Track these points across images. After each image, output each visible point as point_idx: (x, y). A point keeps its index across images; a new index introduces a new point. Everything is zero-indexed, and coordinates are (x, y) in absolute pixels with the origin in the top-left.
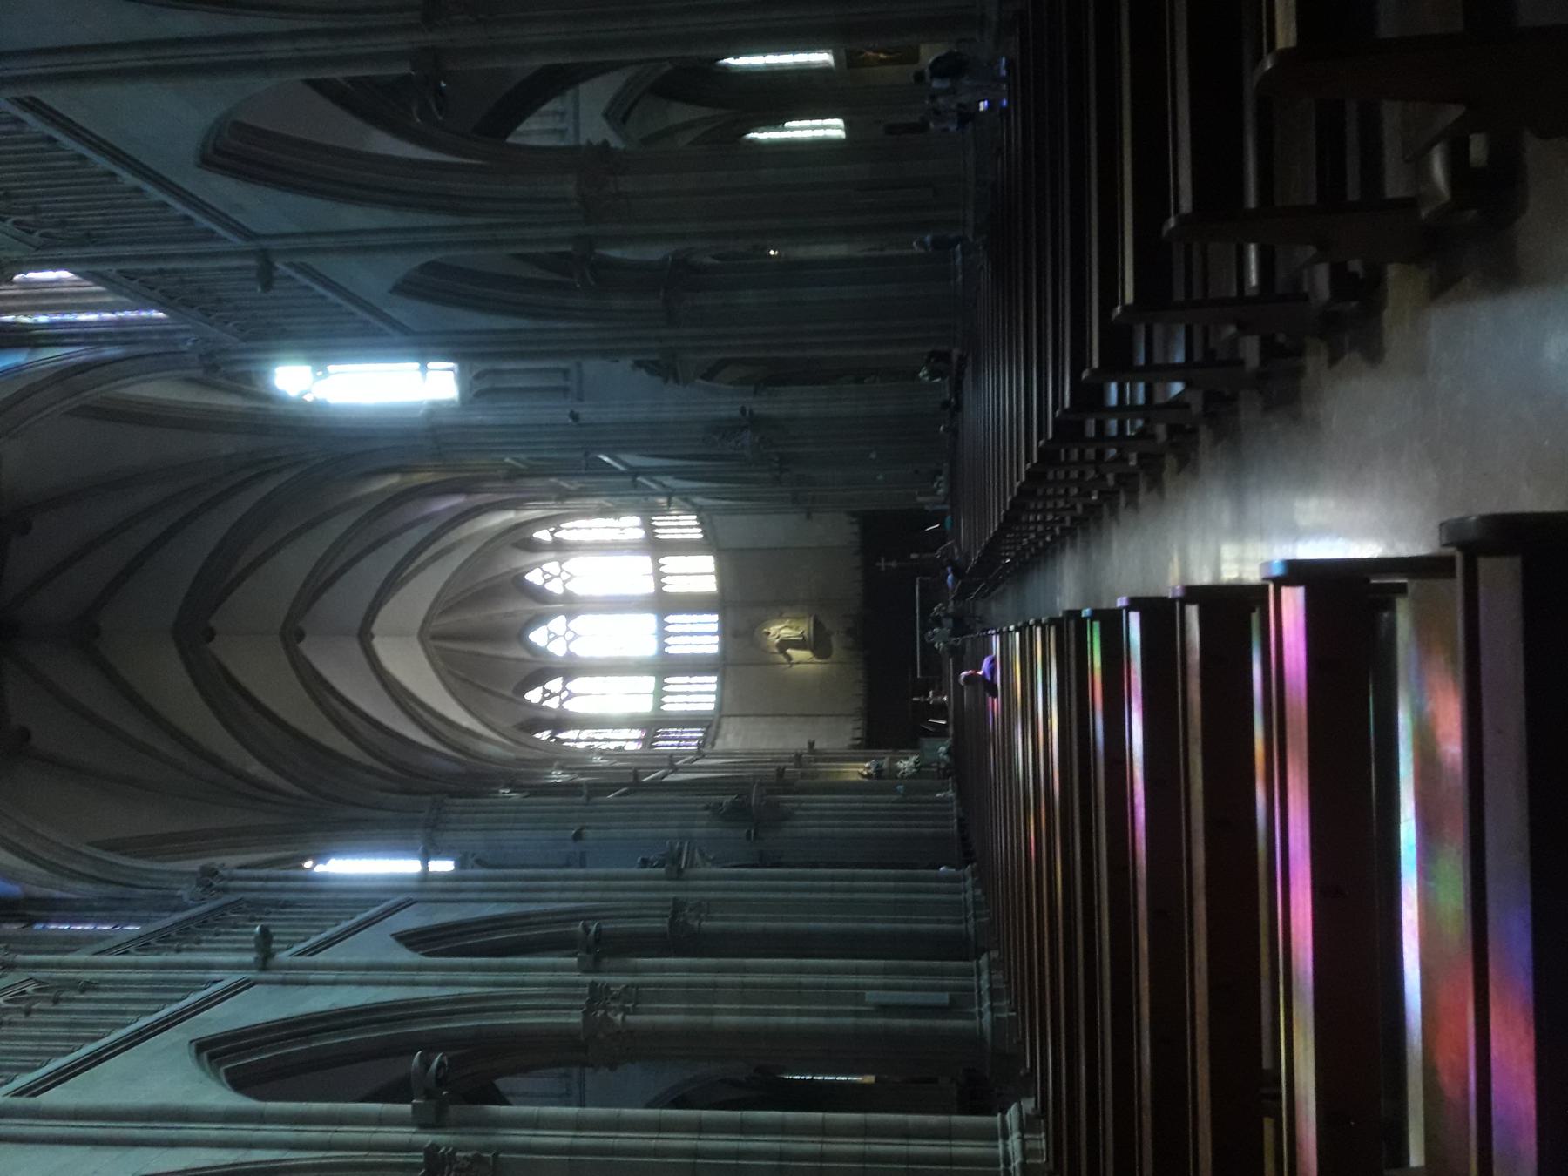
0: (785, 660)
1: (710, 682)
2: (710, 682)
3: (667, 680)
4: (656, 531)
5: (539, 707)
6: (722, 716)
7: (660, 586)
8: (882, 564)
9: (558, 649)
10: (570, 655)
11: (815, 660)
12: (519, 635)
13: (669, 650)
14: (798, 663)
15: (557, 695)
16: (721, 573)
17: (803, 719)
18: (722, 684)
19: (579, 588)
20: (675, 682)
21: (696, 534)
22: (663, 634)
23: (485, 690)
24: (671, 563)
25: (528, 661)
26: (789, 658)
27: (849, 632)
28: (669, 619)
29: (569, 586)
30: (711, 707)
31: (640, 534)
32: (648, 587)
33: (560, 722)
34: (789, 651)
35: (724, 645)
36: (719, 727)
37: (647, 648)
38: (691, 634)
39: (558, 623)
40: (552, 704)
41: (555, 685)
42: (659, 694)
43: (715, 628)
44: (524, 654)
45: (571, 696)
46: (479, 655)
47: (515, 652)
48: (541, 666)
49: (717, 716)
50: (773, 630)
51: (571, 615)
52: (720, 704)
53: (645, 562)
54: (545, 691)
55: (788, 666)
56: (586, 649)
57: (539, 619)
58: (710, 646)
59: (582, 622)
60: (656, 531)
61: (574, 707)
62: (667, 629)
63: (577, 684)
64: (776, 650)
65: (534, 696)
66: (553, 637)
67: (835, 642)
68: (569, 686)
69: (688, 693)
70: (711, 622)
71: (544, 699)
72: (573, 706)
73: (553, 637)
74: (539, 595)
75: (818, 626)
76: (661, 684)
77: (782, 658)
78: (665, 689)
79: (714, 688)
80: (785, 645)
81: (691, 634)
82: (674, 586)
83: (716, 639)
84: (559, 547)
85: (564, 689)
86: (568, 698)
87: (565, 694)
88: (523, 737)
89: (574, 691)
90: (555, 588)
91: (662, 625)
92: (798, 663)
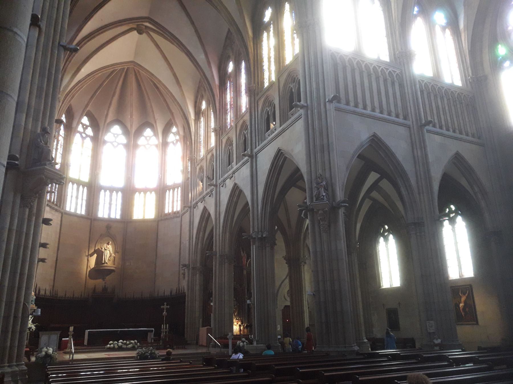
0: (90, 253)
1: (82, 211)
2: (82, 211)
3: (86, 188)
4: (171, 191)
5: (79, 122)
6: (62, 213)
7: (140, 191)
8: (165, 307)
9: (108, 137)
10: (105, 142)
11: (89, 270)
12: (118, 121)
13: (102, 192)
14: (88, 260)
15: (84, 131)
16: (144, 222)
17: (55, 259)
18: (81, 217)
19: (139, 152)
20: (84, 192)
21: (168, 209)
22: (112, 190)
23: (92, 97)
25: (105, 122)
26: (92, 255)
27: (105, 289)
28: (120, 194)
30: (68, 209)
32: (138, 184)
33: (70, 129)
34: (95, 255)
35: (103, 220)
36: (56, 210)
37: (104, 180)
38: (110, 204)
39: (123, 139)
40: (80, 128)
41: (90, 131)
42: (79, 183)
43: (113, 216)
44: (109, 120)
45: (83, 138)
46: (113, 96)
47: (111, 116)
48: (101, 127)
49: (62, 211)
50: (110, 247)
51: (127, 146)
52: (69, 214)
53: (154, 184)
54: (87, 127)
55: (87, 255)
56: (106, 151)
57: (126, 132)
58: (103, 213)
59: (122, 152)
60: (171, 191)
61: (77, 138)
63: (89, 143)
64: (96, 248)
65: (85, 120)
66: (116, 135)
67: (99, 283)
68: (88, 139)
69: (77, 198)
70: (116, 214)
71: (83, 125)
74: (139, 132)
75: (110, 271)
76: (84, 185)
77: (92, 251)
78: (81, 187)
79: (79, 212)
80: (100, 254)
81: (110, 204)
83: (106, 216)
84: (165, 144)
85: (87, 136)
87: (84, 135)
88: (65, 109)
89: (85, 141)
90: (141, 141)
91: (117, 190)
92: (88, 260)
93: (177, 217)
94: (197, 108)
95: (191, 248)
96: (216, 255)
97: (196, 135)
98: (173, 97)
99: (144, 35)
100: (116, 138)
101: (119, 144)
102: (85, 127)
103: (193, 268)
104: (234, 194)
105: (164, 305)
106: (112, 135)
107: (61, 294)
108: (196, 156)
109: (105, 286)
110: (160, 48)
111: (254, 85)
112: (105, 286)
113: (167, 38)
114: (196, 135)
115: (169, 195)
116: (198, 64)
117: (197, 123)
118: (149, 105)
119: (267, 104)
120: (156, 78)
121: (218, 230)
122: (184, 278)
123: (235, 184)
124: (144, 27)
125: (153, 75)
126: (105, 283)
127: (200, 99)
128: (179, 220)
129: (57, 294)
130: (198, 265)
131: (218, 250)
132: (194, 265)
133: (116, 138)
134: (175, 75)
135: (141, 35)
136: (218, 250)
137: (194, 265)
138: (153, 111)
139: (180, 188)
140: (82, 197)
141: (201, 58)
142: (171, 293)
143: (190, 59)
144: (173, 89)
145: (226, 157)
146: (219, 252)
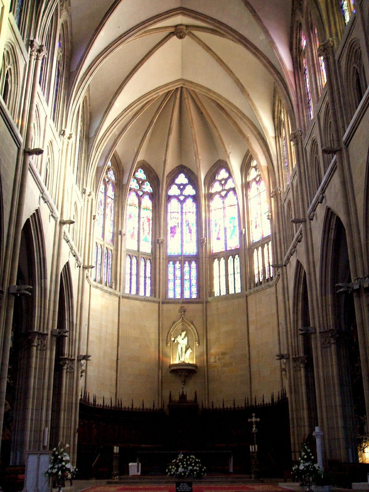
4: (260, 248)
24: (235, 264)
29: (217, 197)
31: (256, 236)
40: (134, 184)
45: (139, 198)
46: (169, 134)
54: (143, 182)
60: (260, 248)
62: (187, 264)
63: (147, 202)
66: (182, 187)
68: (147, 198)
71: (138, 180)
72: (132, 198)
73: (182, 187)
82: (218, 267)
86: (137, 195)
87: (141, 193)
91: (189, 259)
93: (270, 286)
94: (276, 119)
95: (289, 330)
96: (315, 333)
97: (279, 159)
98: (241, 112)
99: (187, 38)
100: (182, 190)
101: (187, 197)
102: (141, 183)
103: (295, 360)
104: (329, 227)
105: (251, 417)
106: (176, 187)
107: (126, 404)
108: (281, 189)
109: (183, 392)
110: (210, 49)
111: (330, 39)
112: (183, 392)
113: (222, 34)
114: (279, 159)
115: (257, 255)
116: (256, 48)
117: (279, 141)
118: (216, 135)
119: (353, 59)
120: (215, 93)
121: (314, 292)
122: (286, 375)
123: (328, 209)
124: (184, 28)
125: (209, 90)
126: (183, 388)
127: (278, 106)
128: (273, 289)
129: (121, 405)
130: (302, 354)
131: (317, 325)
132: (296, 355)
133: (182, 190)
134: (238, 82)
135: (184, 40)
136: (317, 325)
137: (296, 355)
138: (223, 143)
139: (270, 243)
140: (145, 273)
141: (259, 39)
142: (272, 399)
143: (246, 46)
144: (237, 100)
145: (314, 173)
146: (320, 327)
